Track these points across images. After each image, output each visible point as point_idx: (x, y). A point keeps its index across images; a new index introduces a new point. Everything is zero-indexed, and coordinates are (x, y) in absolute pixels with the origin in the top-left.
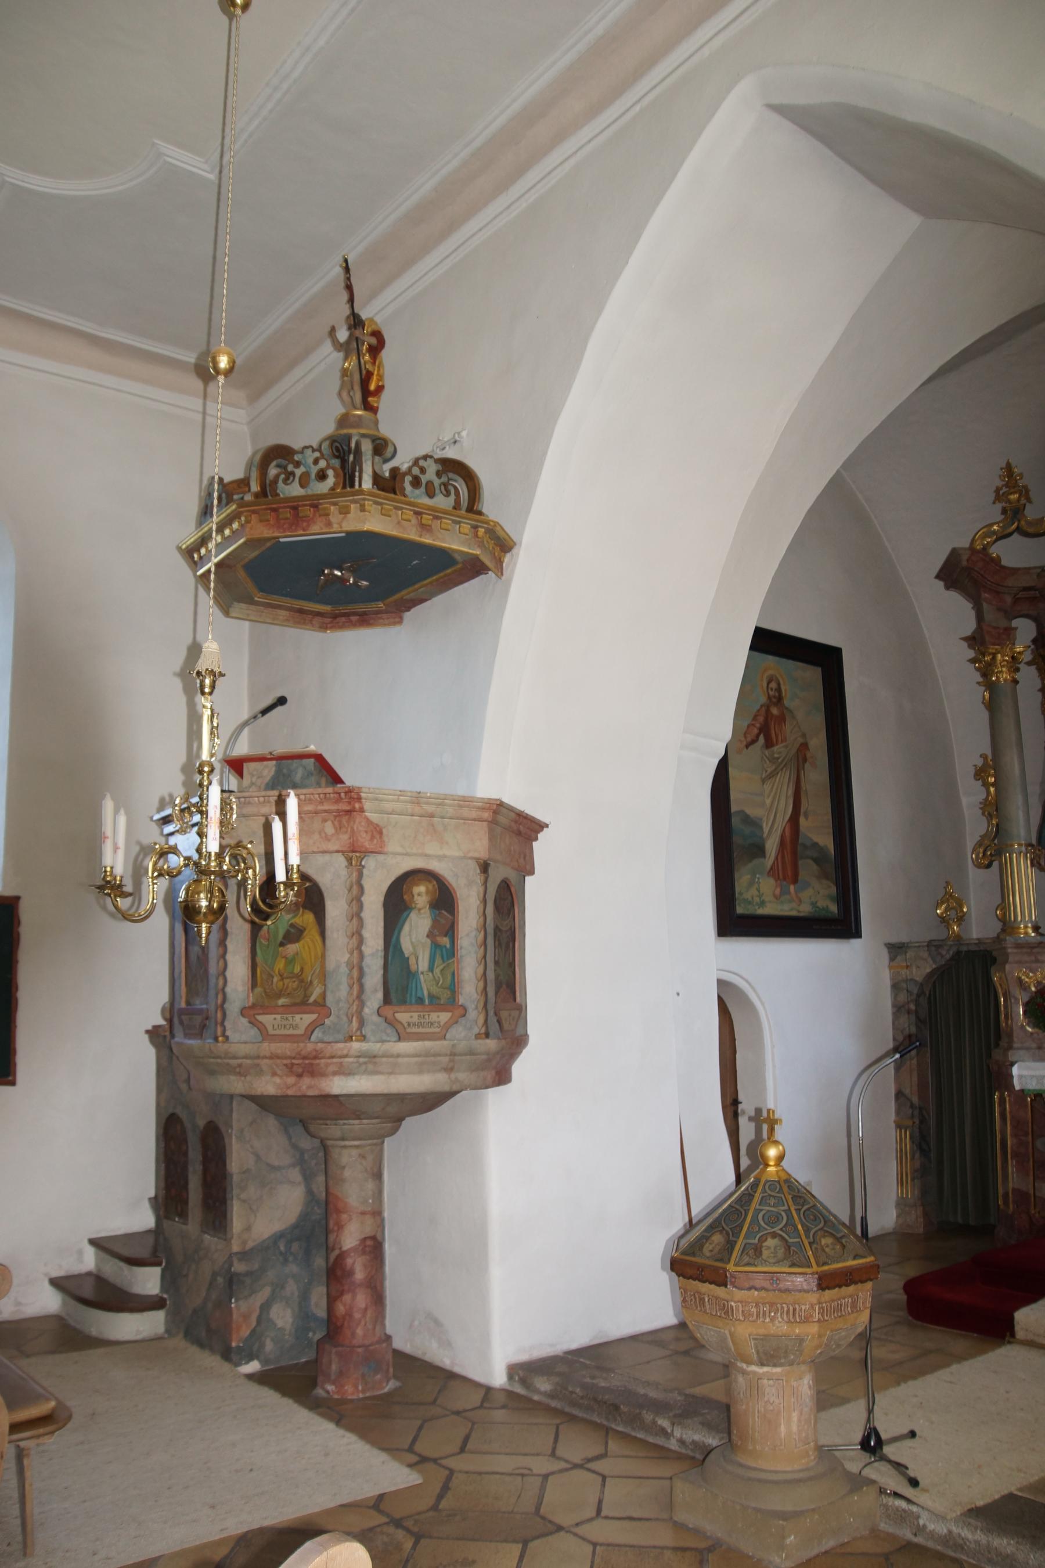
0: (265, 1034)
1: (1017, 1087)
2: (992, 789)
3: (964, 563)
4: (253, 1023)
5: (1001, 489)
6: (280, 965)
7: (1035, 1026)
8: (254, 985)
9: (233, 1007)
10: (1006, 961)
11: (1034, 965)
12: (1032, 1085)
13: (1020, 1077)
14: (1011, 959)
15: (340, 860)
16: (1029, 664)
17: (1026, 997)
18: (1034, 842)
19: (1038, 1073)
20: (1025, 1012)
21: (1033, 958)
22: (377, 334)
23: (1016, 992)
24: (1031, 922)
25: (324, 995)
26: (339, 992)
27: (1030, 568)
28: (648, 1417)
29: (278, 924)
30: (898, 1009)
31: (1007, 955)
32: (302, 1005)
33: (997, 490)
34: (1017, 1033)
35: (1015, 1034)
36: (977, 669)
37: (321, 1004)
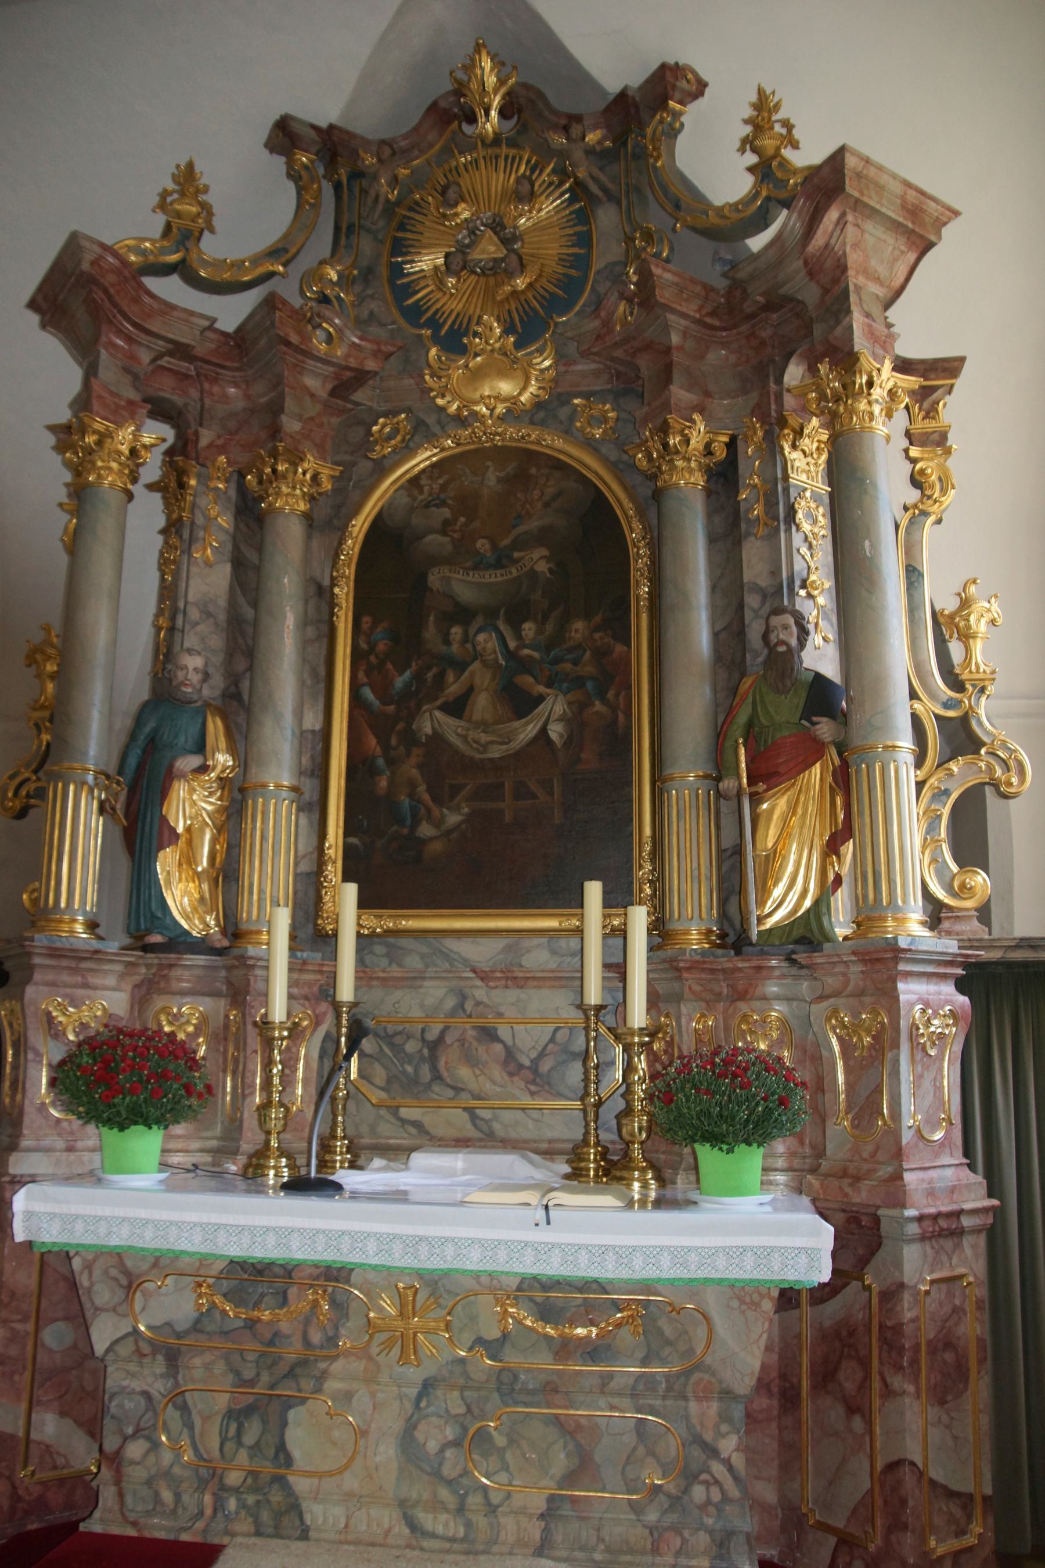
1: (20, 1237)
2: (50, 687)
3: (85, 266)
5: (171, 194)
7: (68, 1108)
10: (28, 980)
11: (80, 992)
12: (50, 1235)
13: (29, 1215)
14: (37, 976)
16: (151, 487)
17: (55, 1053)
18: (112, 770)
19: (65, 1209)
20: (52, 1083)
21: (79, 979)
23: (37, 1038)
24: (85, 913)
27: (192, 313)
31: (31, 969)
33: (164, 194)
34: (30, 1117)
35: (26, 1120)
36: (67, 464)
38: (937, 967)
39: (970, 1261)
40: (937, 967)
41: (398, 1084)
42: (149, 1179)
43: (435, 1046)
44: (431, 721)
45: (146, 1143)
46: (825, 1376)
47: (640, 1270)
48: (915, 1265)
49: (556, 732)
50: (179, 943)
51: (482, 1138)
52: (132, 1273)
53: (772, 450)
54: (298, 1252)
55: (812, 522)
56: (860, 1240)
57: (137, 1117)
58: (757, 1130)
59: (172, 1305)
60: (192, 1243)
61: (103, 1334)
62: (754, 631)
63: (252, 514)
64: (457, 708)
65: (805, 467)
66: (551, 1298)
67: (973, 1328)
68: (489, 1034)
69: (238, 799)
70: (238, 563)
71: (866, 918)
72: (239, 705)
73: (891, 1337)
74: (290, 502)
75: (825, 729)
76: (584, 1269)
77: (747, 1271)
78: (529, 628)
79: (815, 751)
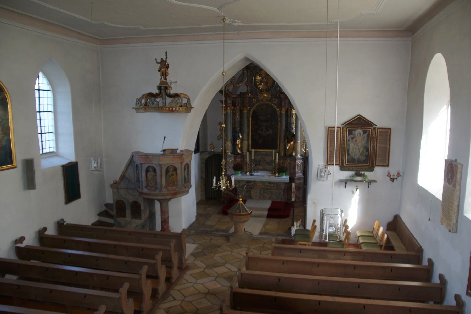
4: (167, 188)
9: (163, 186)
15: (180, 164)
22: (168, 65)
26: (179, 183)
28: (213, 232)
29: (170, 174)
30: (202, 163)
37: (177, 185)
41: (258, 165)
42: (240, 175)
43: (260, 161)
44: (259, 132)
45: (240, 172)
50: (238, 154)
51: (264, 170)
54: (252, 180)
57: (238, 171)
59: (243, 184)
60: (244, 179)
63: (241, 111)
64: (261, 130)
66: (270, 183)
68: (264, 160)
69: (242, 140)
72: (241, 131)
74: (245, 112)
76: (272, 181)
77: (283, 181)
78: (268, 123)
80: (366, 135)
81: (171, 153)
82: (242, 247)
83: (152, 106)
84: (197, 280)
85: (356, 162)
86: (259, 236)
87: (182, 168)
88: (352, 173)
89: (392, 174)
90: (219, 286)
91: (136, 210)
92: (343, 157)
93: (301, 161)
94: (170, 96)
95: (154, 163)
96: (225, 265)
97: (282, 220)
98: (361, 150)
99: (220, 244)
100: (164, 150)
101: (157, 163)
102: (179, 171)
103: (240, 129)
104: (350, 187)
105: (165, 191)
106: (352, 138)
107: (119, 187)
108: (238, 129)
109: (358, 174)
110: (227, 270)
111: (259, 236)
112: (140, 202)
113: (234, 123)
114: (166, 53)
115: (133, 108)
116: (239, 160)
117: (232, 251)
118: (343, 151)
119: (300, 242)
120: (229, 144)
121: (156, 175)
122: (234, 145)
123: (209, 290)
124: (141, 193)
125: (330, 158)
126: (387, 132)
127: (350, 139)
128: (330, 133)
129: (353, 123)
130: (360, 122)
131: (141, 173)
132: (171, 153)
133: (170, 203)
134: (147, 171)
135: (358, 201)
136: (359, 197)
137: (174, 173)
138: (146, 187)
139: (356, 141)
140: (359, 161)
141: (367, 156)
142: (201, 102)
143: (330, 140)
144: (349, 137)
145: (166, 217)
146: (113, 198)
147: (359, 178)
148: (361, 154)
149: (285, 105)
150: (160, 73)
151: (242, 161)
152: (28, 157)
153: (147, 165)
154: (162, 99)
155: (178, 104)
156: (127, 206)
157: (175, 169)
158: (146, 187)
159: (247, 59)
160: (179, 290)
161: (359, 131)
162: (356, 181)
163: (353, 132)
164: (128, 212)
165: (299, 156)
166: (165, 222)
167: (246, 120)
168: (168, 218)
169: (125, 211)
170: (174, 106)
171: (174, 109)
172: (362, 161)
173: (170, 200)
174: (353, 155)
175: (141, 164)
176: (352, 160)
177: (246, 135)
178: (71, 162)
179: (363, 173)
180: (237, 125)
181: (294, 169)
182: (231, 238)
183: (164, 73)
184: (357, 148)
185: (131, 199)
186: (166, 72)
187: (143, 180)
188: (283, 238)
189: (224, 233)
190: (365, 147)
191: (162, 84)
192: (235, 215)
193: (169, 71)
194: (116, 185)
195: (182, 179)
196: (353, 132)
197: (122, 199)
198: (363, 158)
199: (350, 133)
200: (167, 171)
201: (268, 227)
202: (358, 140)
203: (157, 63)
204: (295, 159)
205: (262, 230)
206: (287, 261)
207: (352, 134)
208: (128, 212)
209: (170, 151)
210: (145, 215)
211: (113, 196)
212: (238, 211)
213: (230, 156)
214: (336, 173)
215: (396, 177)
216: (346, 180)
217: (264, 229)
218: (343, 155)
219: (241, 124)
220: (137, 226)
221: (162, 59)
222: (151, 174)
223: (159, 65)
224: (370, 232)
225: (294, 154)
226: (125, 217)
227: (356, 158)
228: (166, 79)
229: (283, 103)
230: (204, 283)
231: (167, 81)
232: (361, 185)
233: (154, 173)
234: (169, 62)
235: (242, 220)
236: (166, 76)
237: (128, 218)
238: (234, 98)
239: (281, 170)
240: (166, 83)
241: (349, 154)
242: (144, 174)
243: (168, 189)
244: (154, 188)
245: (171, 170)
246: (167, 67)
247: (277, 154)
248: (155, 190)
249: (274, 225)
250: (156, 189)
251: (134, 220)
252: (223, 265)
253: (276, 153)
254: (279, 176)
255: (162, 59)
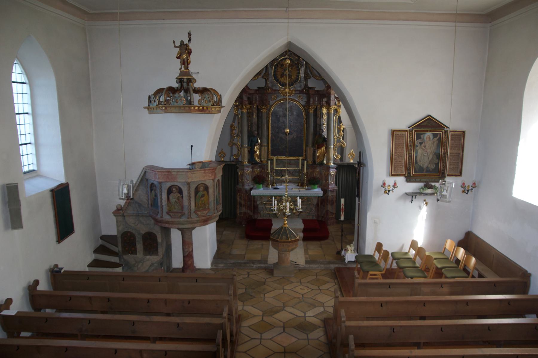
0: (198, 215)
6: (200, 202)
8: (195, 206)
9: (192, 211)
12: (255, 194)
22: (191, 50)
25: (209, 207)
26: (212, 206)
28: (248, 265)
29: (200, 194)
32: (205, 209)
37: (208, 209)
38: (333, 168)
39: (335, 194)
40: (333, 168)
42: (261, 189)
45: (261, 186)
46: (321, 203)
47: (307, 195)
48: (330, 194)
49: (295, 137)
50: (257, 163)
52: (261, 197)
53: (321, 109)
55: (325, 117)
56: (325, 191)
57: (260, 184)
58: (317, 184)
61: (258, 203)
62: (318, 129)
63: (259, 111)
65: (324, 111)
67: (335, 199)
70: (258, 116)
71: (328, 163)
72: (260, 136)
73: (327, 200)
74: (264, 111)
75: (325, 143)
77: (316, 195)
79: (323, 146)
80: (436, 139)
81: (201, 168)
82: (292, 282)
83: (176, 104)
84: (261, 334)
85: (425, 171)
86: (307, 266)
87: (214, 185)
88: (421, 184)
89: (466, 185)
90: (294, 340)
91: (151, 243)
92: (410, 166)
93: (335, 170)
94: (196, 91)
95: (180, 181)
96: (285, 309)
97: (323, 242)
98: (431, 157)
99: (263, 280)
100: (193, 164)
101: (184, 181)
102: (211, 190)
103: (258, 133)
104: (418, 201)
105: (194, 217)
106: (421, 144)
107: (125, 214)
108: (256, 132)
109: (427, 186)
110: (291, 316)
111: (307, 266)
112: (156, 233)
113: (250, 126)
114: (190, 34)
115: (145, 108)
116: (257, 170)
117: (283, 289)
118: (410, 159)
119: (371, 272)
120: (246, 151)
121: (182, 197)
122: (251, 152)
123: (285, 347)
124: (157, 221)
125: (395, 168)
126: (460, 137)
127: (418, 144)
128: (395, 137)
129: (422, 124)
130: (430, 123)
131: (161, 195)
132: (201, 168)
133: (194, 231)
134: (170, 191)
135: (425, 217)
136: (426, 213)
137: (205, 192)
138: (168, 213)
139: (425, 147)
140: (428, 171)
141: (437, 164)
142: (228, 98)
143: (395, 145)
144: (417, 142)
145: (191, 250)
146: (118, 230)
147: (429, 191)
148: (430, 162)
149: (314, 103)
150: (180, 60)
151: (261, 172)
152: (10, 180)
153: (169, 185)
154: (182, 95)
155: (210, 101)
156: (137, 239)
157: (206, 188)
158: (168, 213)
159: (290, 44)
160: (245, 352)
161: (428, 135)
162: (427, 194)
163: (422, 136)
164: (139, 246)
165: (332, 164)
166: (188, 256)
167: (265, 121)
168: (192, 251)
169: (135, 246)
170: (205, 105)
171: (205, 108)
172: (431, 170)
173: (194, 228)
174: (420, 164)
175: (160, 183)
176: (421, 170)
177: (265, 140)
178: (62, 184)
179: (433, 184)
180: (255, 128)
181: (327, 180)
182: (275, 272)
183: (186, 60)
184: (426, 155)
185: (144, 230)
186: (188, 59)
187: (163, 204)
188: (337, 266)
189: (262, 265)
190: (435, 154)
191: (184, 76)
192: (281, 242)
193: (192, 58)
194: (121, 211)
195: (214, 201)
196: (422, 136)
197: (129, 230)
198: (433, 167)
199: (419, 137)
200: (197, 191)
201: (311, 253)
202: (427, 146)
203: (175, 47)
204: (328, 168)
205: (306, 258)
206: (387, 302)
207: (420, 138)
208: (139, 246)
209: (201, 165)
210: (161, 250)
211: (118, 226)
212: (284, 237)
213: (247, 166)
214: (405, 186)
215: (470, 189)
216: (413, 193)
217: (307, 256)
218: (410, 163)
219: (259, 126)
220: (152, 265)
221: (182, 41)
222: (174, 197)
223: (178, 49)
224: (440, 253)
225: (325, 162)
226: (136, 254)
227: (425, 167)
228: (187, 68)
229: (311, 100)
230: (273, 338)
231: (189, 71)
232: (429, 199)
233: (179, 195)
234: (191, 46)
235: (291, 248)
236: (188, 64)
237: (140, 254)
238: (250, 94)
239: (312, 182)
240: (188, 73)
241: (416, 163)
242: (165, 196)
243: (198, 215)
244: (180, 214)
245: (201, 189)
246: (189, 53)
247: (306, 162)
248: (180, 217)
249: (315, 249)
250: (183, 214)
251: (148, 257)
252: (283, 309)
253: (303, 160)
254: (307, 189)
255: (182, 41)
